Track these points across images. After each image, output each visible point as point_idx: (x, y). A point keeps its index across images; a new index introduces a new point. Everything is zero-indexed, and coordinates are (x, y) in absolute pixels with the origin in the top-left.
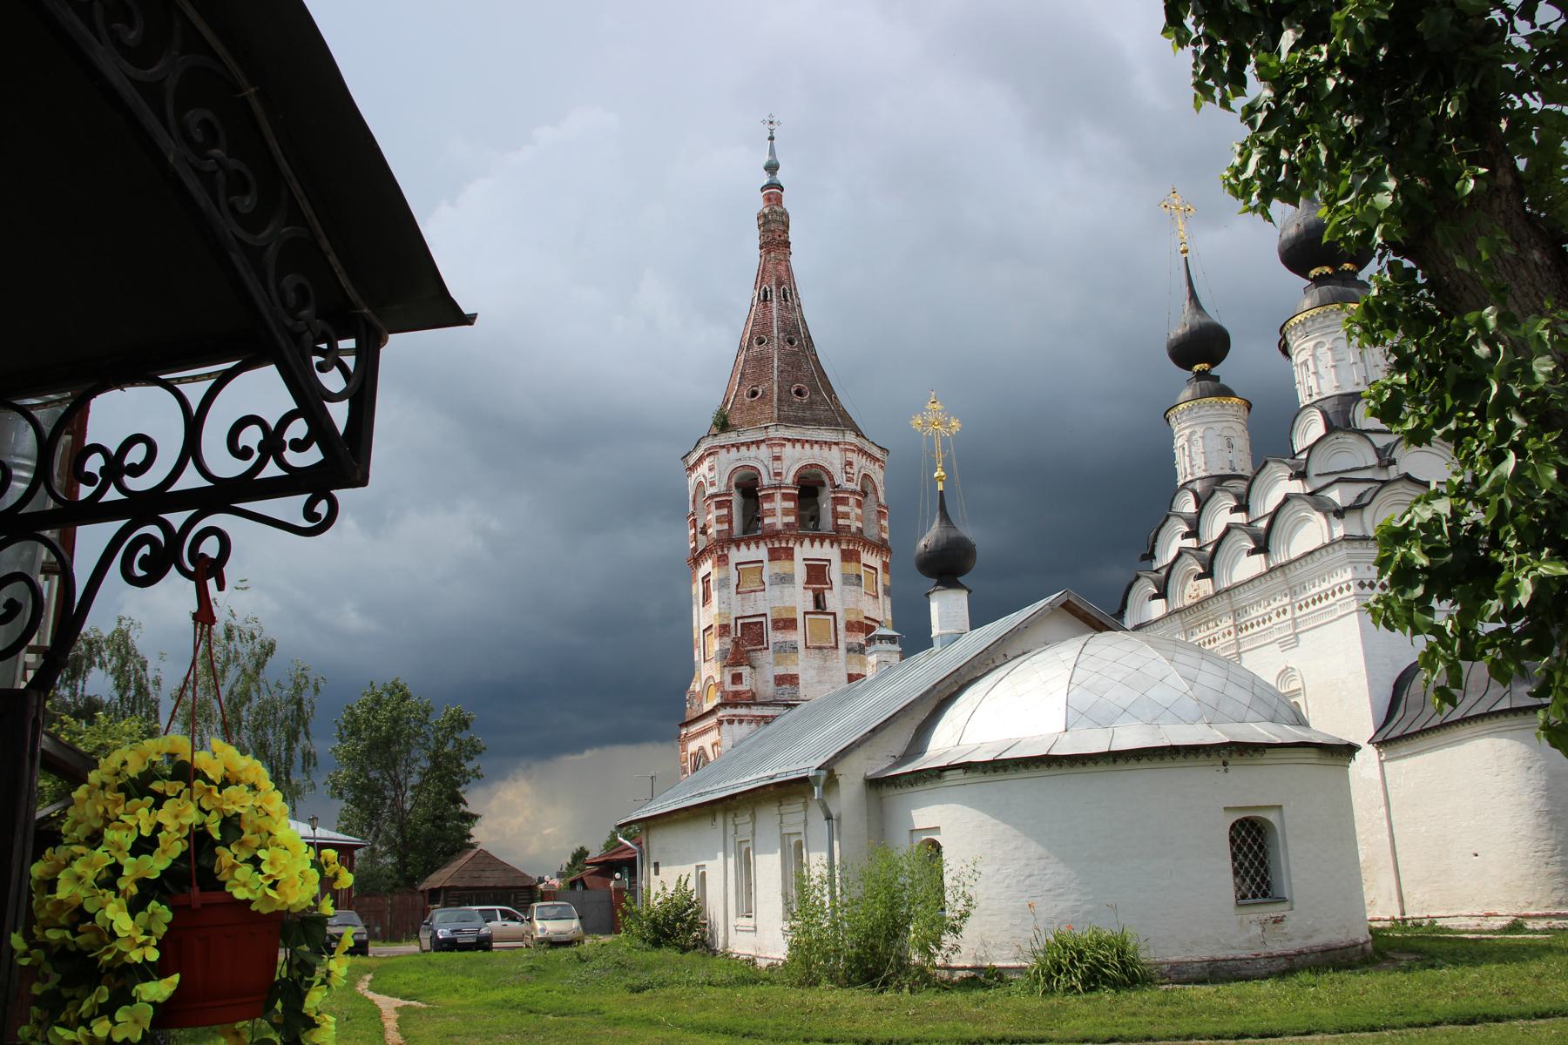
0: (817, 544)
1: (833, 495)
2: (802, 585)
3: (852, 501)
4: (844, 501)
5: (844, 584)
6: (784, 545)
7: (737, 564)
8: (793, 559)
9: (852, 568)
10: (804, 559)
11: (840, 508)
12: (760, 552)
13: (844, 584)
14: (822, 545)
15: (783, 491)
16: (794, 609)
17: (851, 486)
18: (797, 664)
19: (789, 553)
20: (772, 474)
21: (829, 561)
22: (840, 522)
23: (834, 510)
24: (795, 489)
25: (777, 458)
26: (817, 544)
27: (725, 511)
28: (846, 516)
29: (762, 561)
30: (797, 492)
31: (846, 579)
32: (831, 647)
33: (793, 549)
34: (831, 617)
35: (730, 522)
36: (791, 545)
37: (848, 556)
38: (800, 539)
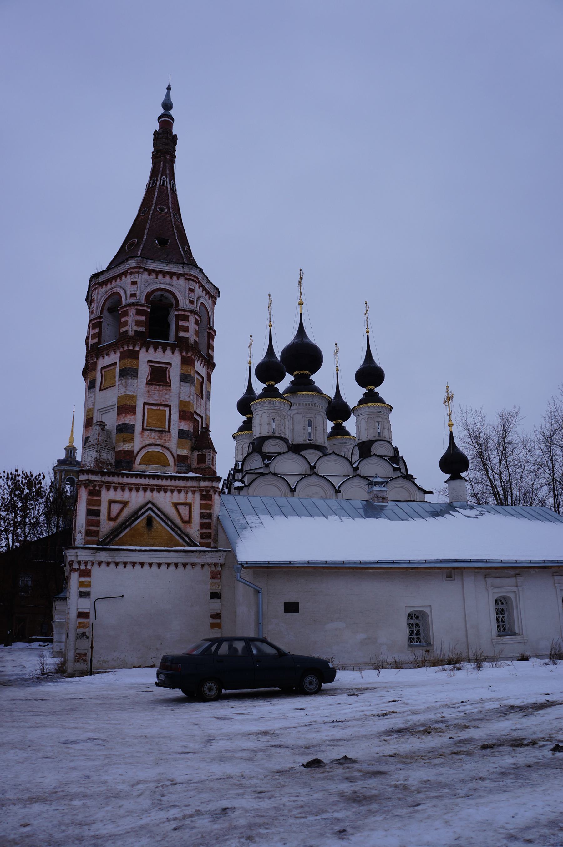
0: (160, 350)
1: (176, 313)
2: (145, 381)
3: (192, 319)
4: (186, 318)
5: (181, 381)
6: (131, 348)
7: (102, 368)
8: (138, 359)
9: (188, 370)
10: (149, 361)
11: (181, 323)
12: (114, 357)
13: (182, 380)
14: (164, 352)
15: (136, 307)
16: (134, 397)
17: (190, 306)
18: (132, 440)
19: (135, 356)
20: (128, 296)
21: (170, 364)
22: (182, 334)
23: (177, 325)
24: (147, 307)
25: (134, 283)
26: (160, 350)
27: (97, 330)
28: (186, 329)
29: (115, 364)
30: (149, 310)
31: (185, 378)
32: (165, 431)
33: (138, 351)
34: (167, 409)
35: (99, 335)
36: (137, 348)
37: (186, 362)
38: (147, 346)
